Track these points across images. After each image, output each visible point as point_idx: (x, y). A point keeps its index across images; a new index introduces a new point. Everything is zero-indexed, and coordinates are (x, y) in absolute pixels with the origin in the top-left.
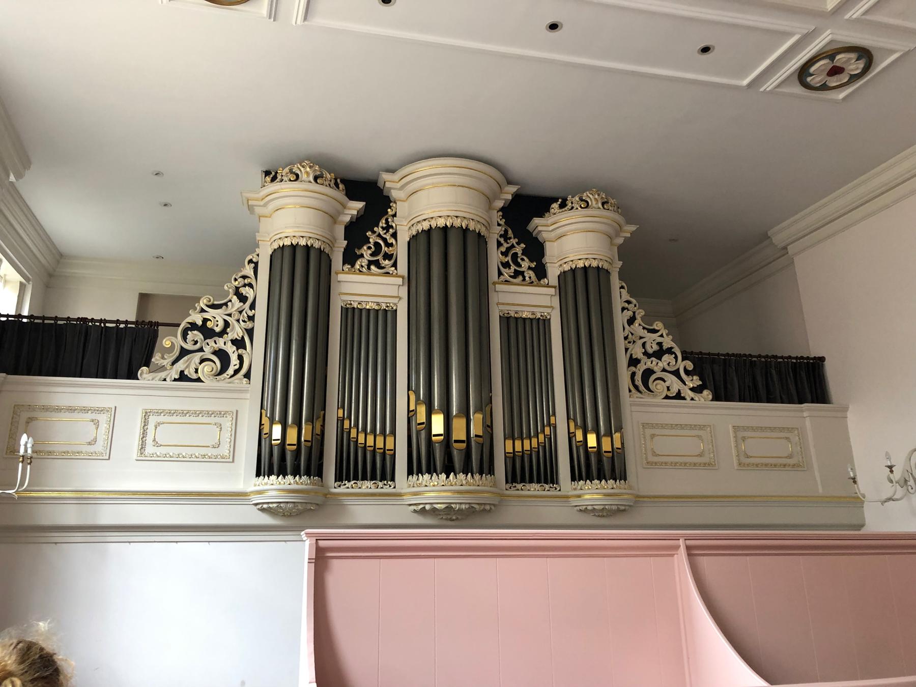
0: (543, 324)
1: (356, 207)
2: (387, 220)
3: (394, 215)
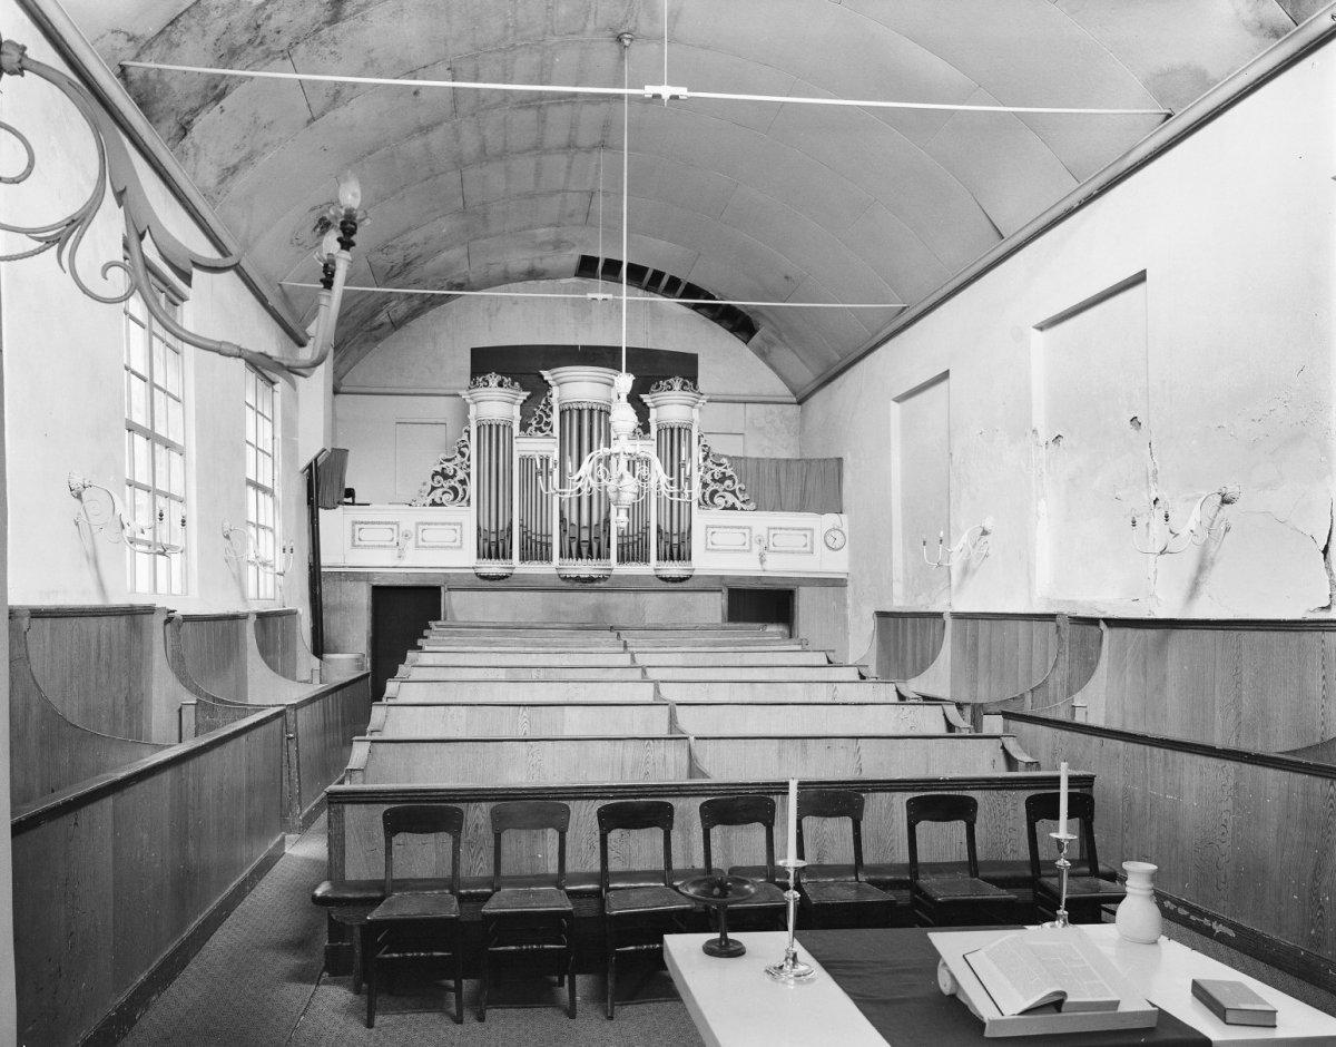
1: (524, 395)
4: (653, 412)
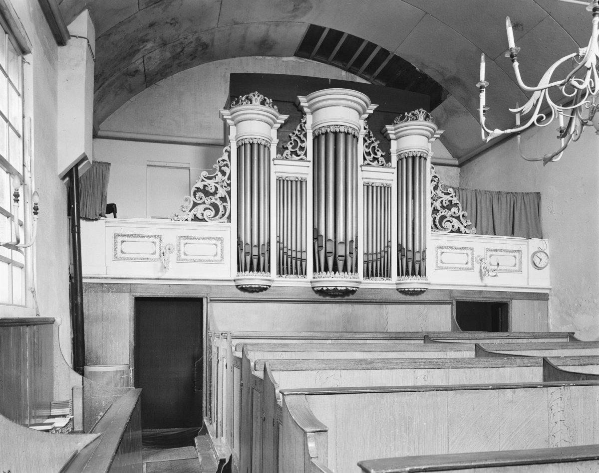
0: (389, 187)
2: (301, 125)
3: (305, 123)
4: (394, 144)
